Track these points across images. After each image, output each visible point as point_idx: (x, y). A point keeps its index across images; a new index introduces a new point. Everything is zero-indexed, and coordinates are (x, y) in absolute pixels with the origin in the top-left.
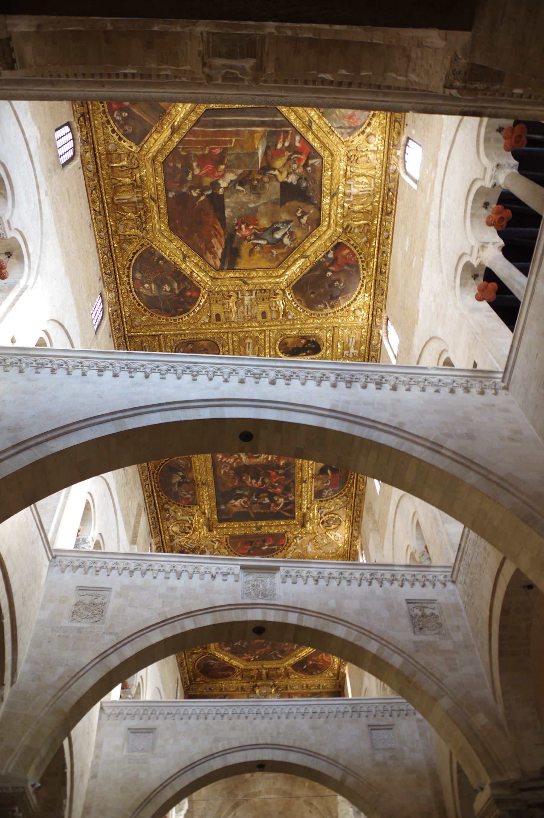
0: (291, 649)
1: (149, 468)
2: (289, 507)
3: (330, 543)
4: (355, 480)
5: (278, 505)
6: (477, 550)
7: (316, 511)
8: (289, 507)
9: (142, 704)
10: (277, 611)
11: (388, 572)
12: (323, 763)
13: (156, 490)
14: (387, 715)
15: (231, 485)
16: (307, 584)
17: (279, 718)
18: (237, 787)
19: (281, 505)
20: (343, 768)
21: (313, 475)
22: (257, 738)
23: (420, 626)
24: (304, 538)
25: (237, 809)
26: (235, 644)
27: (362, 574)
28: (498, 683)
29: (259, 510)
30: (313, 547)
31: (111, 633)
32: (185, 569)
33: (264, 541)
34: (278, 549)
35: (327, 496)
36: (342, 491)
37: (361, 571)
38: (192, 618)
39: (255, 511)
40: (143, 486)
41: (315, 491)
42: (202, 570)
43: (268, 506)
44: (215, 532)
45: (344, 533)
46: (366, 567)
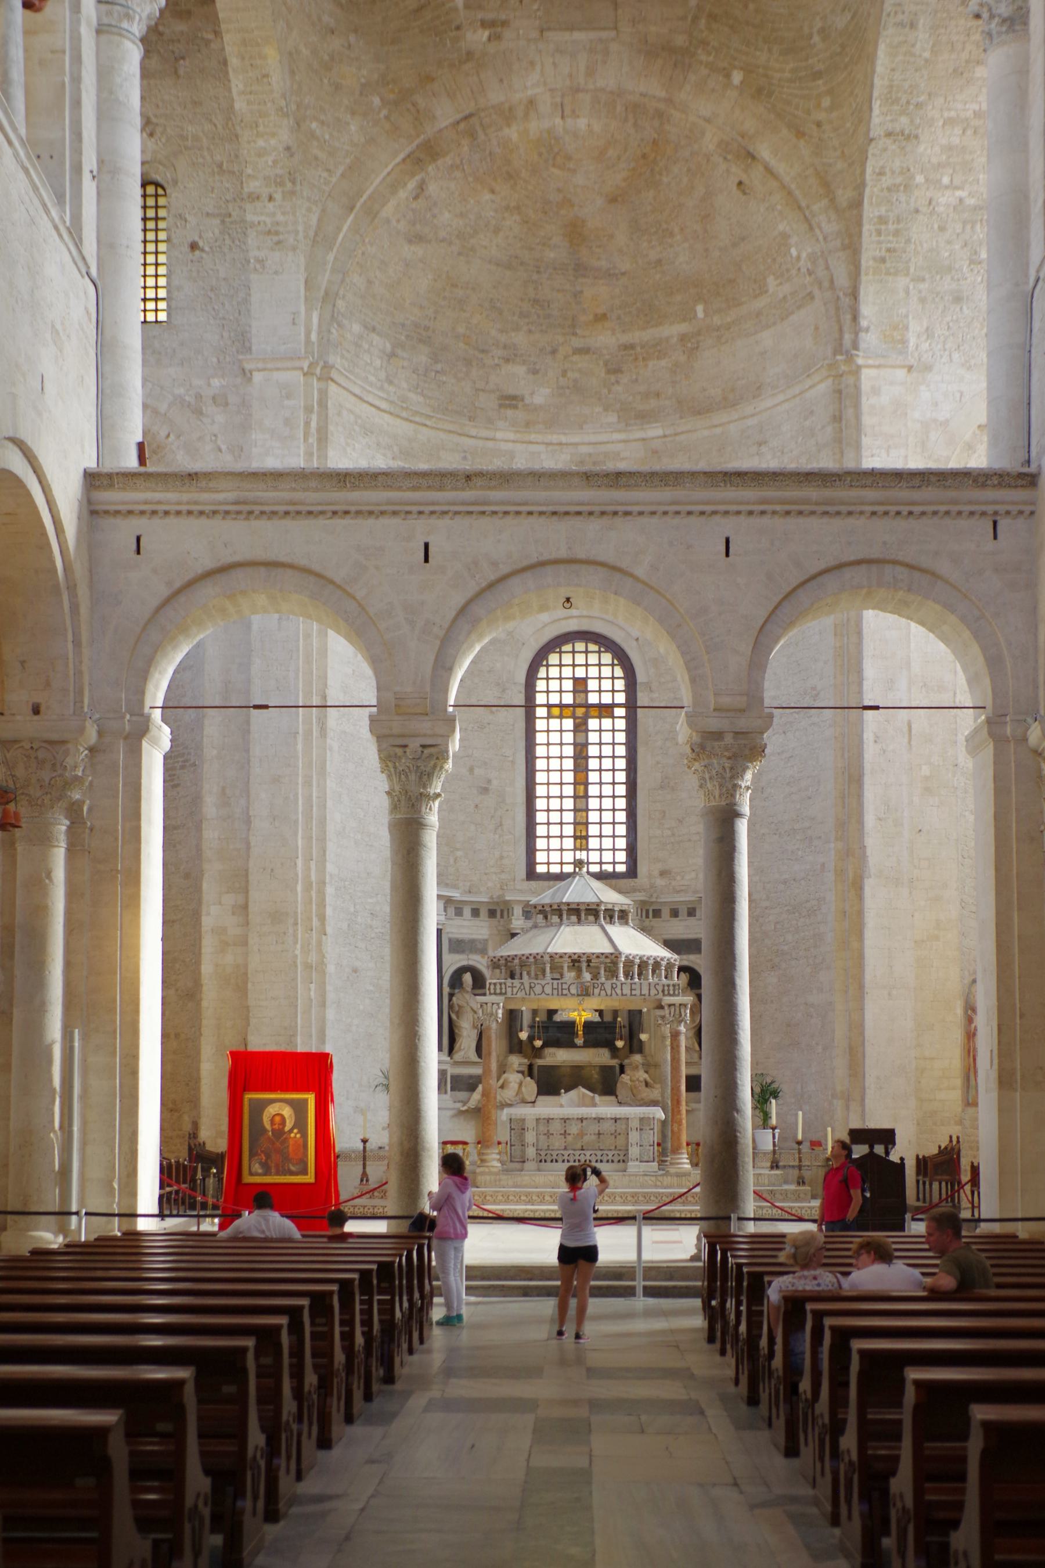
18: (430, 79)
25: (431, 168)
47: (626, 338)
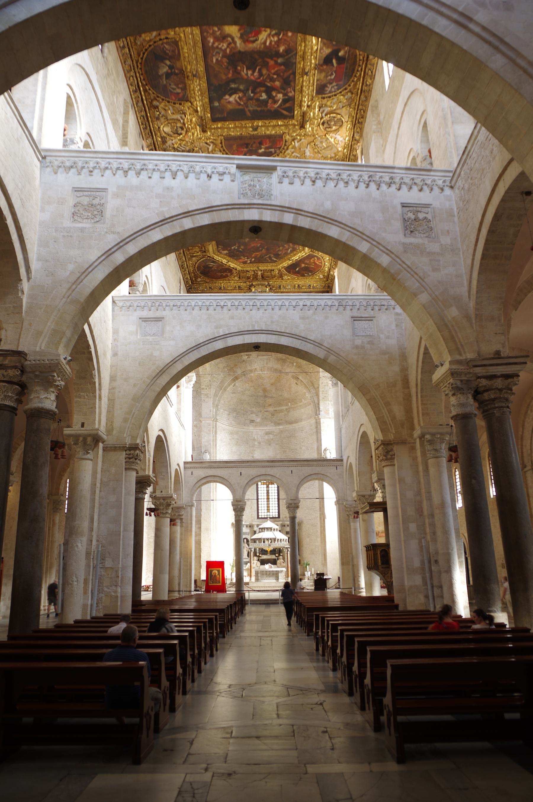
0: (285, 253)
1: (131, 55)
2: (287, 105)
3: (330, 146)
4: (362, 73)
5: (275, 102)
6: (483, 153)
7: (317, 110)
8: (287, 105)
9: (149, 298)
10: (273, 211)
11: (387, 174)
12: (309, 345)
13: (142, 83)
14: (370, 308)
15: (224, 77)
16: (304, 185)
17: (273, 309)
19: (280, 102)
20: (327, 349)
21: (316, 65)
22: (253, 326)
23: (411, 230)
24: (302, 140)
26: (233, 248)
27: (361, 176)
28: (474, 283)
29: (255, 108)
30: (311, 150)
31: (114, 233)
32: (180, 168)
33: (261, 143)
34: (275, 152)
35: (330, 92)
36: (347, 86)
37: (360, 173)
38: (189, 217)
39: (251, 109)
40: (128, 80)
41: (317, 85)
42: (198, 169)
44: (209, 133)
45: (344, 135)
46: (365, 169)
47: (275, 409)
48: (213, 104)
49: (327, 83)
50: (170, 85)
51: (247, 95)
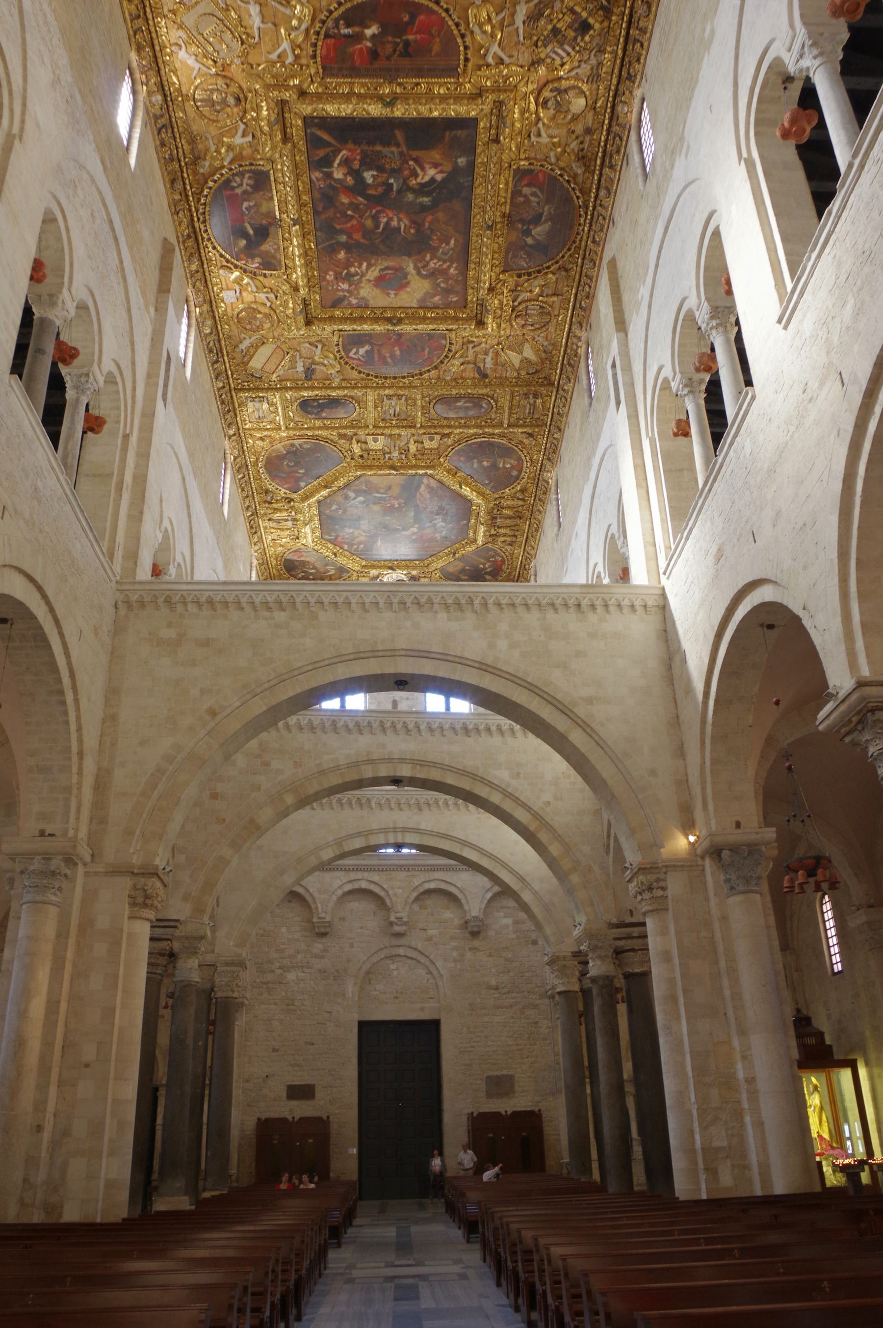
2: (321, 153)
5: (346, 162)
8: (321, 153)
15: (440, 215)
19: (337, 161)
24: (274, 56)
29: (385, 150)
33: (374, 54)
34: (337, 21)
35: (242, 174)
39: (393, 149)
41: (271, 190)
43: (368, 162)
48: (467, 161)
49: (252, 193)
50: (538, 203)
51: (401, 181)
